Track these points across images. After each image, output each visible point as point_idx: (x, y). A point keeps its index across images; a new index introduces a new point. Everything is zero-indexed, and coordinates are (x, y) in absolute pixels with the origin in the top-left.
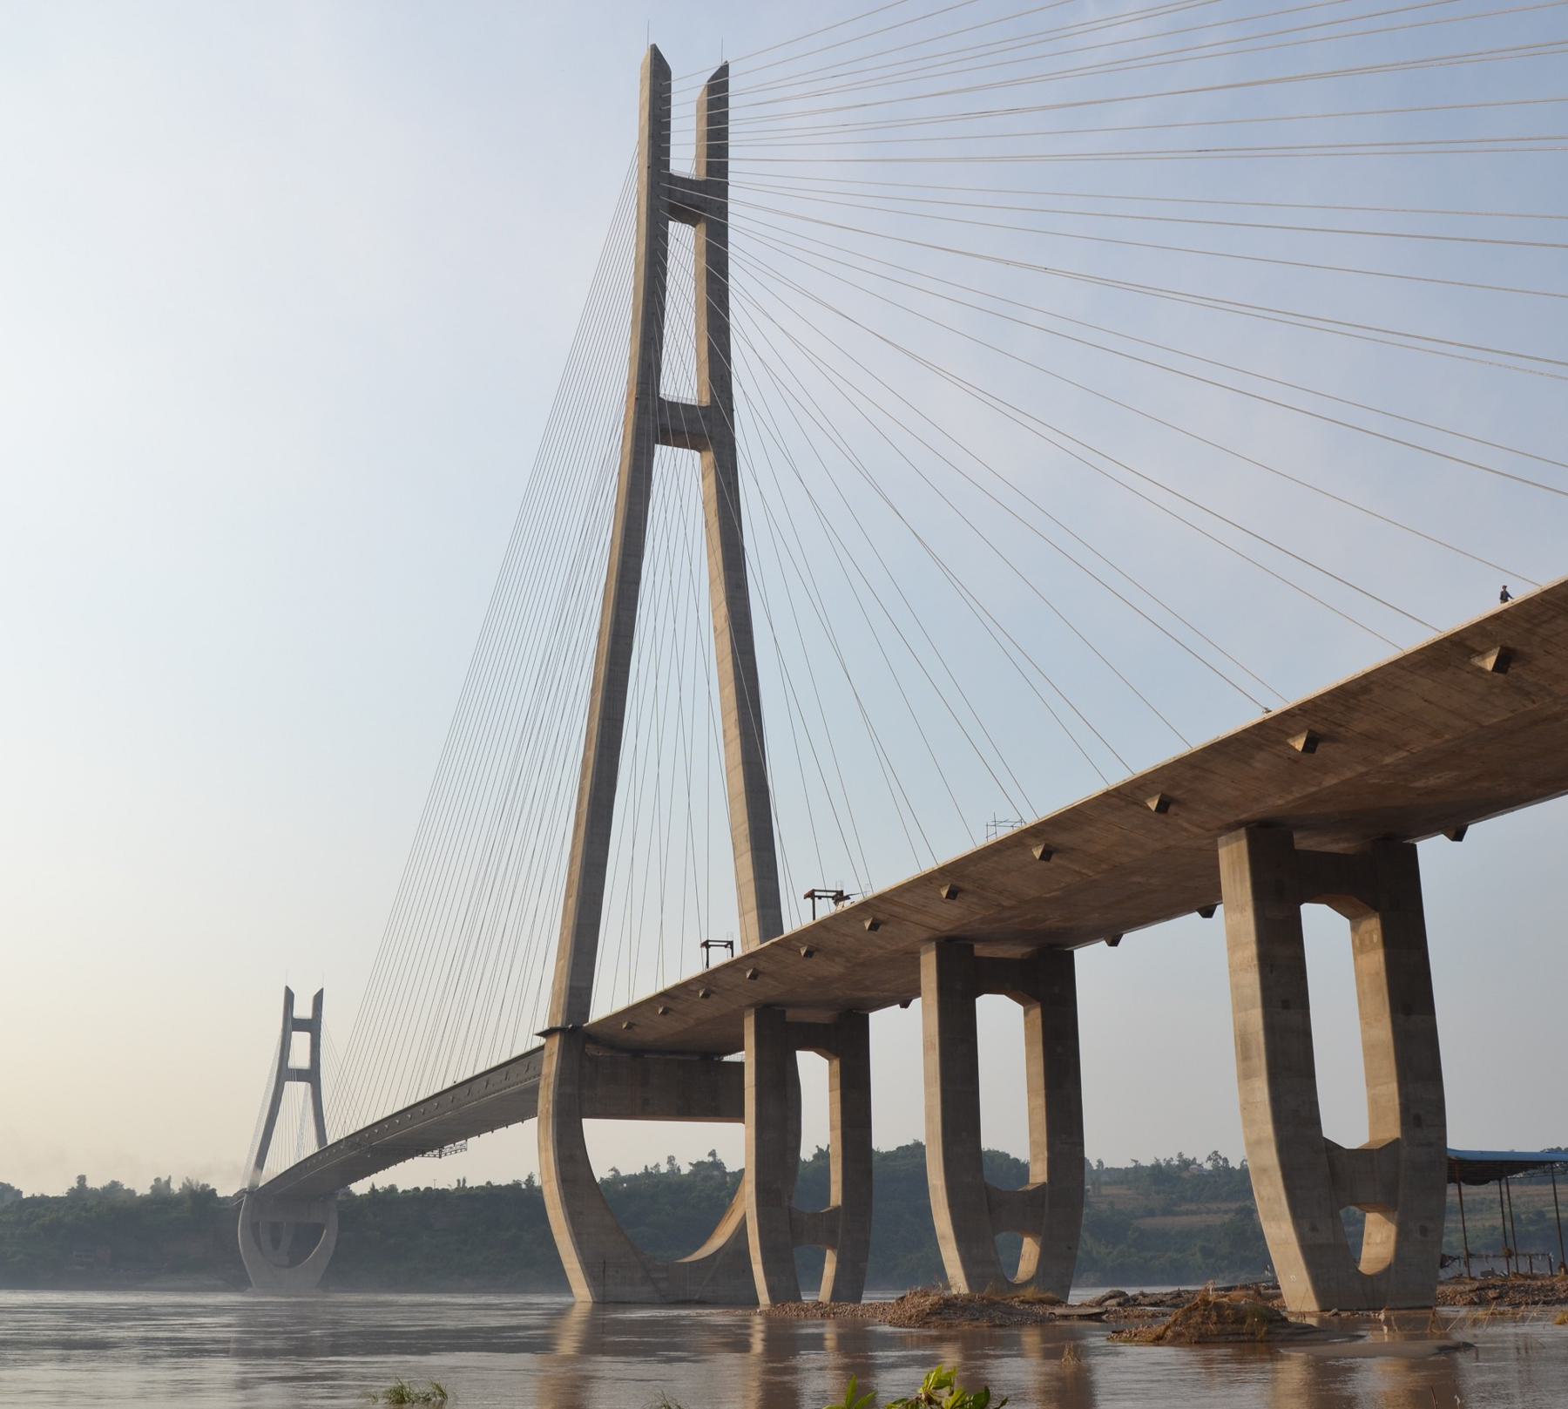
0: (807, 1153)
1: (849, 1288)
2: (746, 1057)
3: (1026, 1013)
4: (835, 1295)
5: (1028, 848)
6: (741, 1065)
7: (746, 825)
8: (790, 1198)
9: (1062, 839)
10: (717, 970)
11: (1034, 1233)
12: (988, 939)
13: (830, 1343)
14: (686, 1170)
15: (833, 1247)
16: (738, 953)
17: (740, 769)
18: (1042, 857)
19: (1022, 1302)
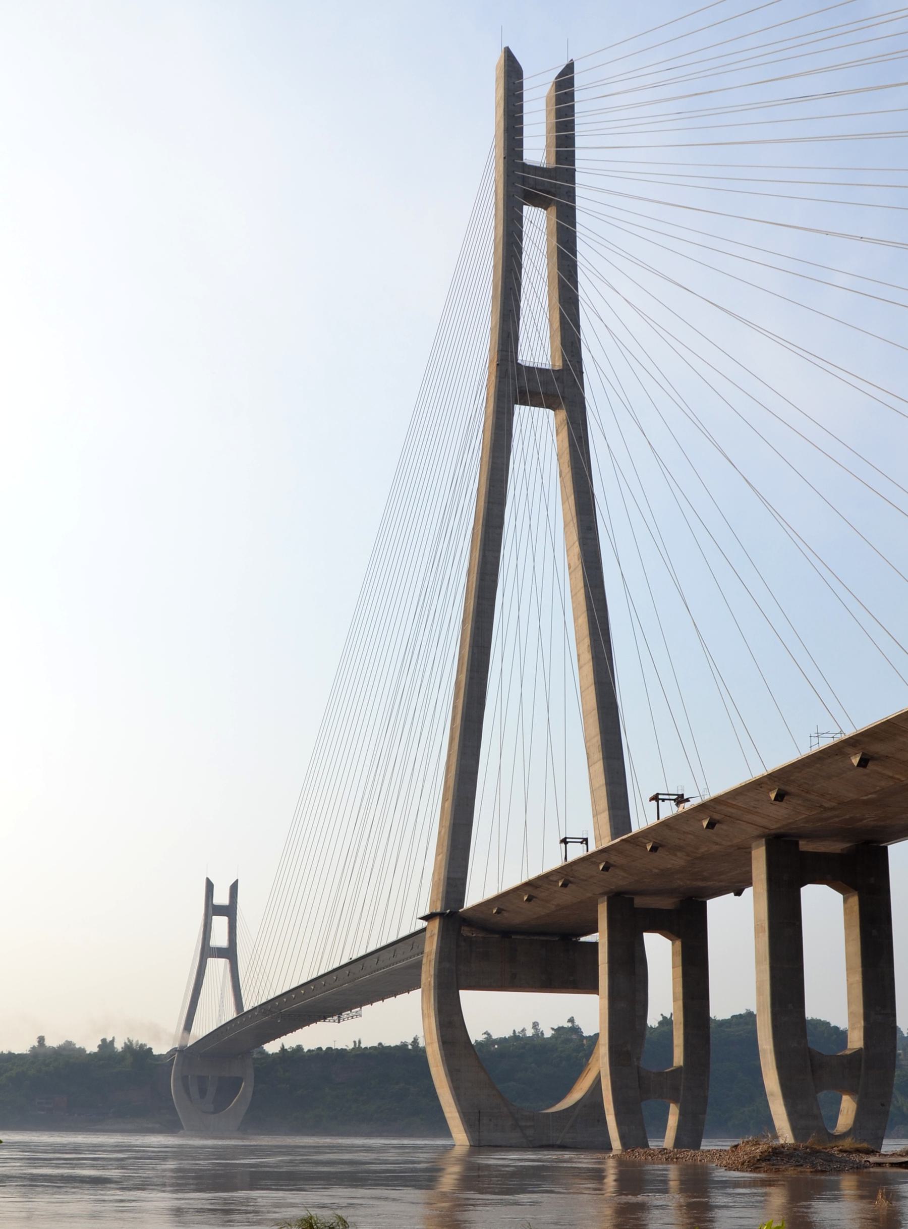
0: (653, 1020)
1: (689, 1136)
2: (599, 938)
3: (845, 901)
4: (678, 1143)
5: (847, 756)
6: (595, 945)
7: (598, 738)
8: (638, 1059)
9: (877, 748)
10: (575, 863)
11: (851, 1092)
12: (811, 836)
13: (673, 1185)
14: (548, 1034)
15: (676, 1101)
16: (593, 848)
17: (592, 689)
18: (859, 764)
19: (841, 1151)
